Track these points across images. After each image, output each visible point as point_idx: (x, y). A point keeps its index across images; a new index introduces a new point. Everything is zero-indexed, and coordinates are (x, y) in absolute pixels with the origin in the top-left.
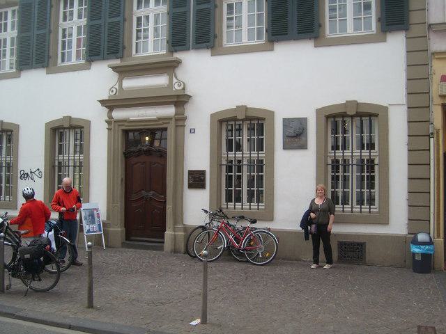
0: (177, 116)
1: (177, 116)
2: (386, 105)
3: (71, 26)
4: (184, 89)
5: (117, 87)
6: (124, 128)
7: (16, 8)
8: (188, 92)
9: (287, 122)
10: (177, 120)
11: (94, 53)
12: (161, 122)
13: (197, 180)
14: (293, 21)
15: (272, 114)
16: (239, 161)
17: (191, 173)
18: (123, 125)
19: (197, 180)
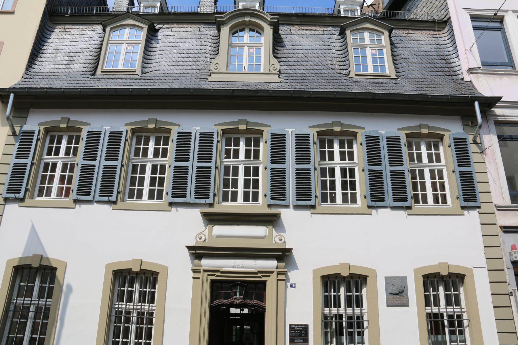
0: (278, 270)
1: (278, 270)
3: (143, 163)
5: (206, 233)
9: (389, 280)
12: (260, 275)
15: (375, 271)
16: (358, 318)
18: (214, 275)
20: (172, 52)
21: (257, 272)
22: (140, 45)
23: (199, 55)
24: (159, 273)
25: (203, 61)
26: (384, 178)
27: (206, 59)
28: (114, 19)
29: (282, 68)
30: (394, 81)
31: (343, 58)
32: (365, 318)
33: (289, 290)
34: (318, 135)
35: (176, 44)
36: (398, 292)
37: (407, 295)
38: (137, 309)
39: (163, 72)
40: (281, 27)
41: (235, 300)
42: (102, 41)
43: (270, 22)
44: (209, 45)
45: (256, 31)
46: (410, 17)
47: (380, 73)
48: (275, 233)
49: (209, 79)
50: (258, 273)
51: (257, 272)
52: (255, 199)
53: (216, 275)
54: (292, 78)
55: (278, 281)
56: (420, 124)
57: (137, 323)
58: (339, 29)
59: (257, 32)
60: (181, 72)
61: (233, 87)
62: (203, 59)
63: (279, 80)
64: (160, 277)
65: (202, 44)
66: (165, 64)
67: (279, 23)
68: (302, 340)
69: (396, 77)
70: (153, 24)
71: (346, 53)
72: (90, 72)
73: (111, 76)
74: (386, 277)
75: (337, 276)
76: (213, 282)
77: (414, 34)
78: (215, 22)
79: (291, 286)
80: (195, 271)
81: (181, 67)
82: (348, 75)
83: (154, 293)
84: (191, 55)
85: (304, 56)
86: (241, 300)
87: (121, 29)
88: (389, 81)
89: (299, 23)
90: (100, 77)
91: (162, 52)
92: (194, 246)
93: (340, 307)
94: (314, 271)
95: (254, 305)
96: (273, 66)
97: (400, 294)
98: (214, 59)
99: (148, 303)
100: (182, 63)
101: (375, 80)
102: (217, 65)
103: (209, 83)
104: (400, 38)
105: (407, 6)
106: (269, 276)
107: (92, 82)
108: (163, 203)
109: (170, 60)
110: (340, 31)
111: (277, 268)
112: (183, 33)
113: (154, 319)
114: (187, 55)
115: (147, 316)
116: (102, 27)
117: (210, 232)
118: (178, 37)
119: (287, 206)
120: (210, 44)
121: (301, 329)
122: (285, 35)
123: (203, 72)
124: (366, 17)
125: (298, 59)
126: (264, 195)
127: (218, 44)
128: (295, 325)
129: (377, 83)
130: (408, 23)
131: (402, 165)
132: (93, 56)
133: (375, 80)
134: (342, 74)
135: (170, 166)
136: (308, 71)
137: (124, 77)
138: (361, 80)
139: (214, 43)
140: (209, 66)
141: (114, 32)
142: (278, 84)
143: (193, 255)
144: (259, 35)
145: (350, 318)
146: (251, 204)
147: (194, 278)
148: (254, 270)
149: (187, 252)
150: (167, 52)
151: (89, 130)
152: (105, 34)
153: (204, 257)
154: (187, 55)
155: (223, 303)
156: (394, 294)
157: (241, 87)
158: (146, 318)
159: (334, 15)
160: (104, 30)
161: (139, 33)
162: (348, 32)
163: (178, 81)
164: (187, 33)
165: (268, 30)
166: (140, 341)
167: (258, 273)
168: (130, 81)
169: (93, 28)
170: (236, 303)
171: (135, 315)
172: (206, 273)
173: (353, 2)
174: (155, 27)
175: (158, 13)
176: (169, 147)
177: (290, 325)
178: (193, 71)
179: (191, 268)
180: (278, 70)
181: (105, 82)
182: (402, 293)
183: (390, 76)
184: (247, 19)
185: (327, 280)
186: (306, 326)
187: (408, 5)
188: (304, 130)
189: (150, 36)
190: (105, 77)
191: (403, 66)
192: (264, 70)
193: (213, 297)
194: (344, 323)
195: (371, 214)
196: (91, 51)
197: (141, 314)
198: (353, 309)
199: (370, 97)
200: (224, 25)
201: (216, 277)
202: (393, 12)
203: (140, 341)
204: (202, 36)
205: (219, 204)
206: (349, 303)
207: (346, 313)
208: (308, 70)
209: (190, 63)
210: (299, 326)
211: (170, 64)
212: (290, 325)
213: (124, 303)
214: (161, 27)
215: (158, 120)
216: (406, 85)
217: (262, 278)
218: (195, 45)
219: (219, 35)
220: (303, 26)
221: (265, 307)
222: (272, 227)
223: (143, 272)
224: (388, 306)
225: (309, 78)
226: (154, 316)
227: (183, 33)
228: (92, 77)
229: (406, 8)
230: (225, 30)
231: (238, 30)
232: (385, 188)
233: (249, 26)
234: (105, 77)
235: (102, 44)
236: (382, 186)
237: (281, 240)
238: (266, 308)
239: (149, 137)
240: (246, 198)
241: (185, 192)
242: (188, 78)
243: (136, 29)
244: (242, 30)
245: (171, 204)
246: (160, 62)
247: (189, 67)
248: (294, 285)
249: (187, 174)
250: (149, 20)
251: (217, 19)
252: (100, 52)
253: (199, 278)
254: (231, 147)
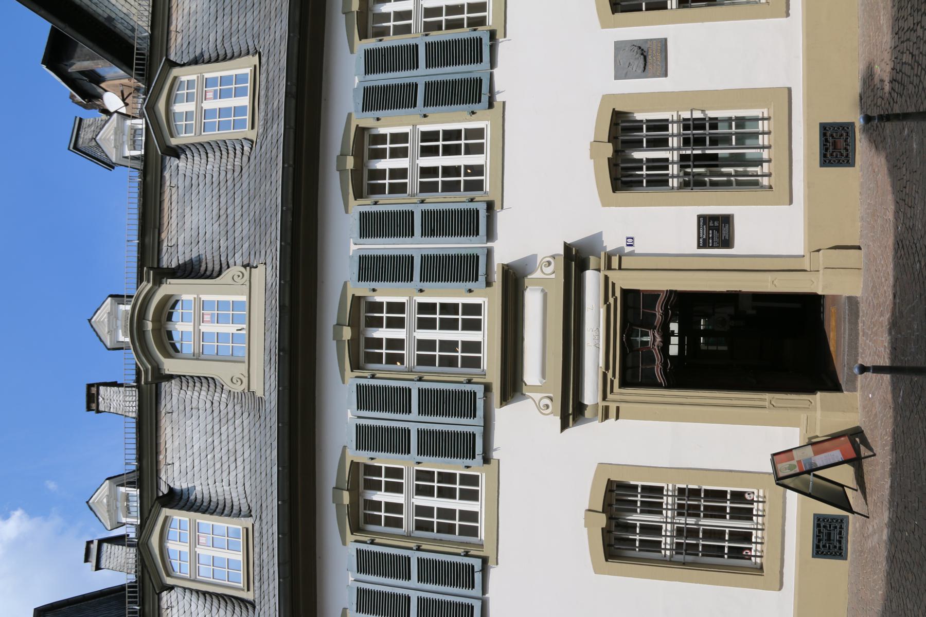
0: (602, 267)
1: (602, 267)
5: (537, 396)
6: (616, 382)
12: (611, 300)
15: (606, 98)
16: (686, 127)
18: (612, 382)
20: (211, 463)
21: (606, 305)
22: (198, 521)
23: (216, 413)
24: (609, 480)
25: (227, 405)
26: (439, 78)
27: (223, 400)
28: (150, 570)
29: (239, 262)
30: (264, 60)
31: (221, 151)
32: (686, 115)
33: (638, 248)
34: (361, 197)
35: (196, 454)
36: (642, 57)
37: (646, 41)
38: (673, 517)
39: (247, 477)
40: (164, 264)
41: (656, 344)
42: (191, 590)
43: (154, 284)
44: (197, 394)
45: (171, 309)
46: (146, 28)
47: (248, 85)
48: (537, 274)
49: (259, 394)
50: (608, 303)
51: (606, 305)
52: (475, 309)
53: (613, 379)
54: (257, 244)
55: (622, 268)
56: (343, 13)
57: (698, 516)
58: (168, 158)
59: (173, 307)
60: (247, 446)
61: (275, 351)
62: (223, 407)
63: (262, 268)
64: (617, 477)
65: (195, 408)
66: (233, 474)
67: (156, 266)
68: (725, 227)
69: (257, 55)
70: (158, 498)
71: (211, 145)
72: (249, 610)
73: (255, 573)
74: (616, 78)
75: (613, 164)
76: (624, 384)
77: (178, 21)
78: (154, 385)
79: (631, 245)
80: (606, 416)
81: (239, 446)
82: (252, 142)
83: (644, 488)
84: (216, 428)
85: (218, 223)
86: (656, 334)
87: (169, 558)
88: (265, 67)
89: (157, 231)
90: (257, 592)
91: (211, 481)
92: (561, 418)
93: (667, 160)
94: (604, 205)
95: (664, 311)
96: (236, 278)
97: (645, 54)
98: (223, 386)
99: (662, 498)
100: (231, 444)
101: (263, 93)
102: (234, 381)
103: (267, 394)
104: (185, 46)
105: (126, 32)
106: (613, 284)
107: (267, 607)
108: (484, 475)
109: (225, 466)
110: (170, 155)
111: (599, 270)
112: (176, 443)
113: (690, 486)
114: (216, 435)
115: (684, 500)
116: (165, 592)
117: (535, 389)
118: (183, 452)
119: (489, 253)
120: (196, 394)
121: (706, 228)
122: (178, 257)
123: (247, 405)
124: (145, 108)
125: (223, 233)
126: (469, 294)
127: (195, 378)
128: (699, 238)
129: (267, 89)
130: (156, 33)
131: (417, 46)
132: (219, 607)
133: (263, 93)
134: (250, 154)
135: (419, 463)
136: (245, 216)
137: (257, 550)
138: (261, 119)
139: (194, 386)
140: (236, 394)
141: (174, 571)
142: (269, 269)
143: (576, 419)
144: (179, 305)
145: (686, 142)
146: (485, 317)
147: (617, 418)
149: (572, 431)
150: (211, 471)
151: (356, 609)
152: (178, 586)
153: (580, 400)
154: (216, 435)
155: (661, 365)
156: (645, 65)
157: (274, 335)
158: (689, 500)
159: (142, 168)
160: (171, 588)
161: (175, 524)
162: (174, 142)
163: (263, 451)
164: (176, 435)
165: (170, 287)
166: (728, 511)
167: (608, 303)
168: (265, 537)
169: (167, 609)
170: (661, 341)
171: (682, 520)
172: (609, 396)
173: (118, 133)
174: (164, 495)
175: (138, 490)
176: (383, 465)
177: (699, 247)
178: (246, 423)
179: (599, 422)
180: (243, 269)
181: (266, 583)
182: (642, 50)
183: (255, 66)
184: (149, 326)
185: (620, 181)
186: (701, 219)
187: (123, 31)
188: (352, 222)
189: (182, 504)
190: (257, 584)
191: (236, 43)
192: (242, 295)
193: (650, 382)
194: (695, 152)
195: (504, 103)
196: (211, 611)
197: (681, 510)
198: (670, 136)
199: (293, 102)
200: (160, 367)
201: (615, 378)
202: (137, 59)
203: (728, 511)
204: (182, 408)
205: (485, 375)
206: (662, 143)
207: (679, 149)
208: (242, 215)
209: (231, 429)
210: (701, 231)
211: (233, 467)
212: (699, 247)
213: (663, 539)
214: (164, 483)
215: (335, 486)
216: (271, 37)
217: (616, 298)
218: (198, 421)
219: (180, 376)
220: (161, 224)
221: (667, 291)
222: (526, 280)
223: (607, 507)
224: (666, 75)
225: (257, 212)
226: (684, 486)
227: (176, 443)
228: (258, 607)
229: (130, 35)
230: (170, 366)
231: (171, 343)
232: (458, 77)
233: (163, 322)
234: (257, 584)
235: (197, 592)
236: (454, 83)
237: (549, 263)
238: (669, 289)
239: (366, 501)
240: (475, 326)
241: (464, 434)
242: (258, 433)
243: (168, 528)
244: (170, 335)
245: (486, 460)
246: (229, 485)
247: (239, 430)
248: (629, 240)
249: (431, 433)
250: (152, 507)
251: (150, 380)
252: (211, 594)
253: (618, 408)
254: (382, 353)
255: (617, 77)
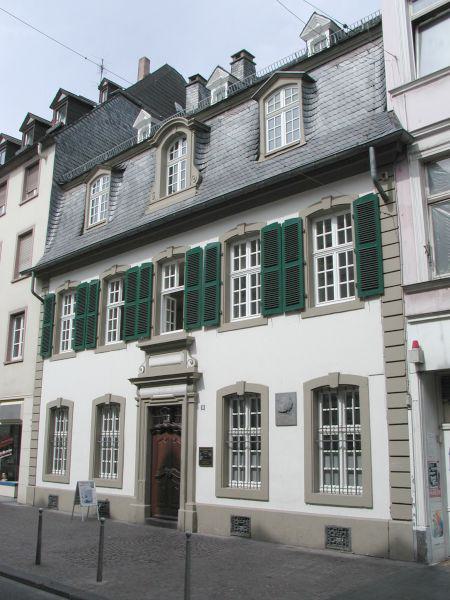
2: (364, 375)
4: (196, 366)
6: (147, 405)
7: (76, 292)
8: (200, 371)
9: (279, 396)
10: (188, 397)
11: (127, 335)
12: (176, 399)
13: (206, 458)
14: (282, 296)
17: (201, 449)
19: (206, 458)
64: (122, 408)
76: (149, 408)
111: (188, 391)
119: (200, 328)
148: (171, 395)
184: (174, 132)
230: (261, 101)
255: (277, 395)
